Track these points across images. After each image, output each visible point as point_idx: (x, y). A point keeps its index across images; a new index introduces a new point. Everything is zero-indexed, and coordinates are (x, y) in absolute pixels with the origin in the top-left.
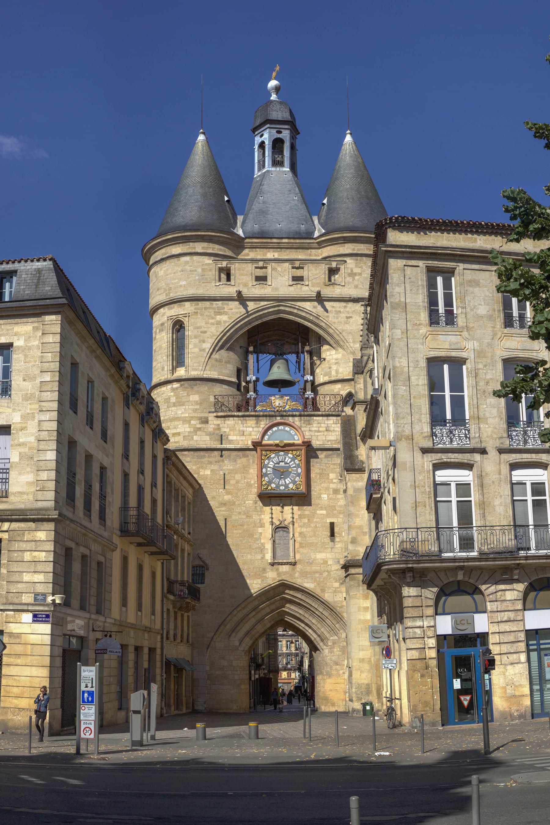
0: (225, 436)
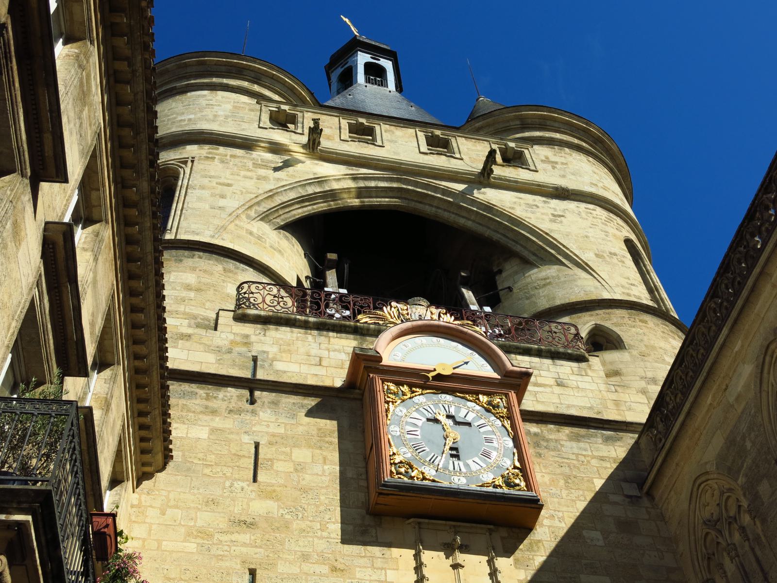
0: (263, 361)
